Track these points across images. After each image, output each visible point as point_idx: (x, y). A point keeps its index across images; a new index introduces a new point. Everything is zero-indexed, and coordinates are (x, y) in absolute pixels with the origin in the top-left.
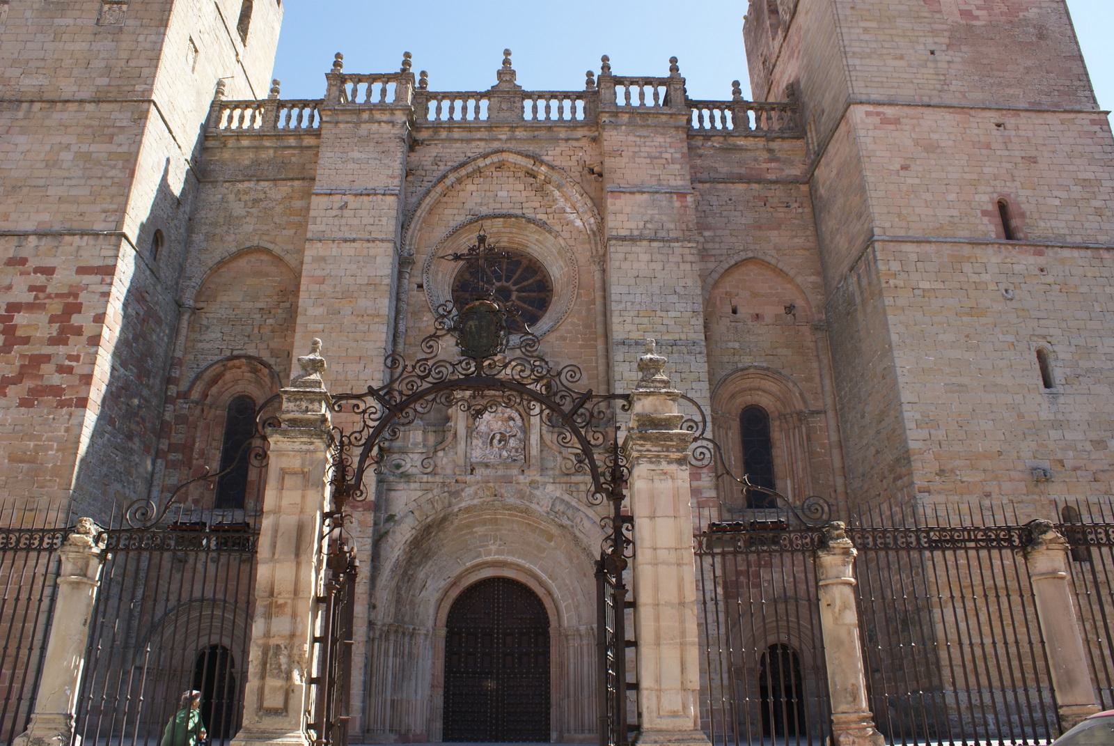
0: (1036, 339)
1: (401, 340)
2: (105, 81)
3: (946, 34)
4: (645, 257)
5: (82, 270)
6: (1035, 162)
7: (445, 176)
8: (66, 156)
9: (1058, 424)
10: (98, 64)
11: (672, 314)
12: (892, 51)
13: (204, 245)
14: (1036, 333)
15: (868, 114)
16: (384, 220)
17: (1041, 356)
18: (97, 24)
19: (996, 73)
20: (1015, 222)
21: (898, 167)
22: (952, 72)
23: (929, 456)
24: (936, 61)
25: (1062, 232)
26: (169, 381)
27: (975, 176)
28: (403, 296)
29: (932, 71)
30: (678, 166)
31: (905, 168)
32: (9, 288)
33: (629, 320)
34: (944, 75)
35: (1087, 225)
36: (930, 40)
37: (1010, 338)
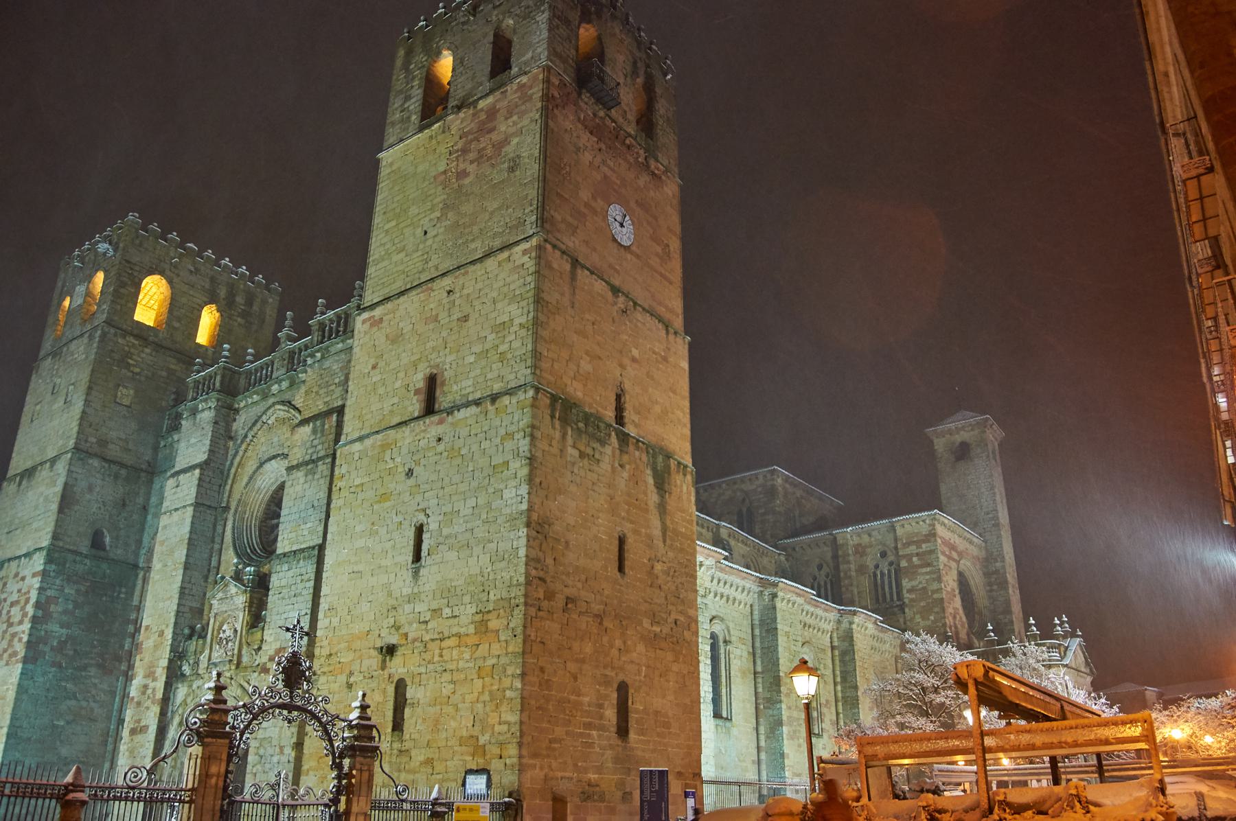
0: (417, 513)
1: (213, 572)
2: (61, 442)
3: (441, 205)
4: (302, 480)
5: (34, 575)
6: (466, 321)
7: (246, 436)
8: (41, 500)
9: (411, 599)
10: (61, 432)
11: (309, 525)
12: (398, 246)
13: (151, 522)
14: (420, 507)
15: (364, 322)
16: (192, 489)
17: (420, 531)
18: (65, 403)
19: (467, 231)
20: (438, 393)
21: (370, 367)
22: (435, 246)
23: (325, 643)
24: (426, 240)
25: (468, 390)
26: (128, 622)
27: (418, 357)
28: (218, 539)
29: (420, 253)
30: (341, 388)
31: (374, 367)
32: (12, 593)
33: (286, 536)
34: (427, 253)
35: (489, 376)
36: (427, 219)
37: (400, 518)
